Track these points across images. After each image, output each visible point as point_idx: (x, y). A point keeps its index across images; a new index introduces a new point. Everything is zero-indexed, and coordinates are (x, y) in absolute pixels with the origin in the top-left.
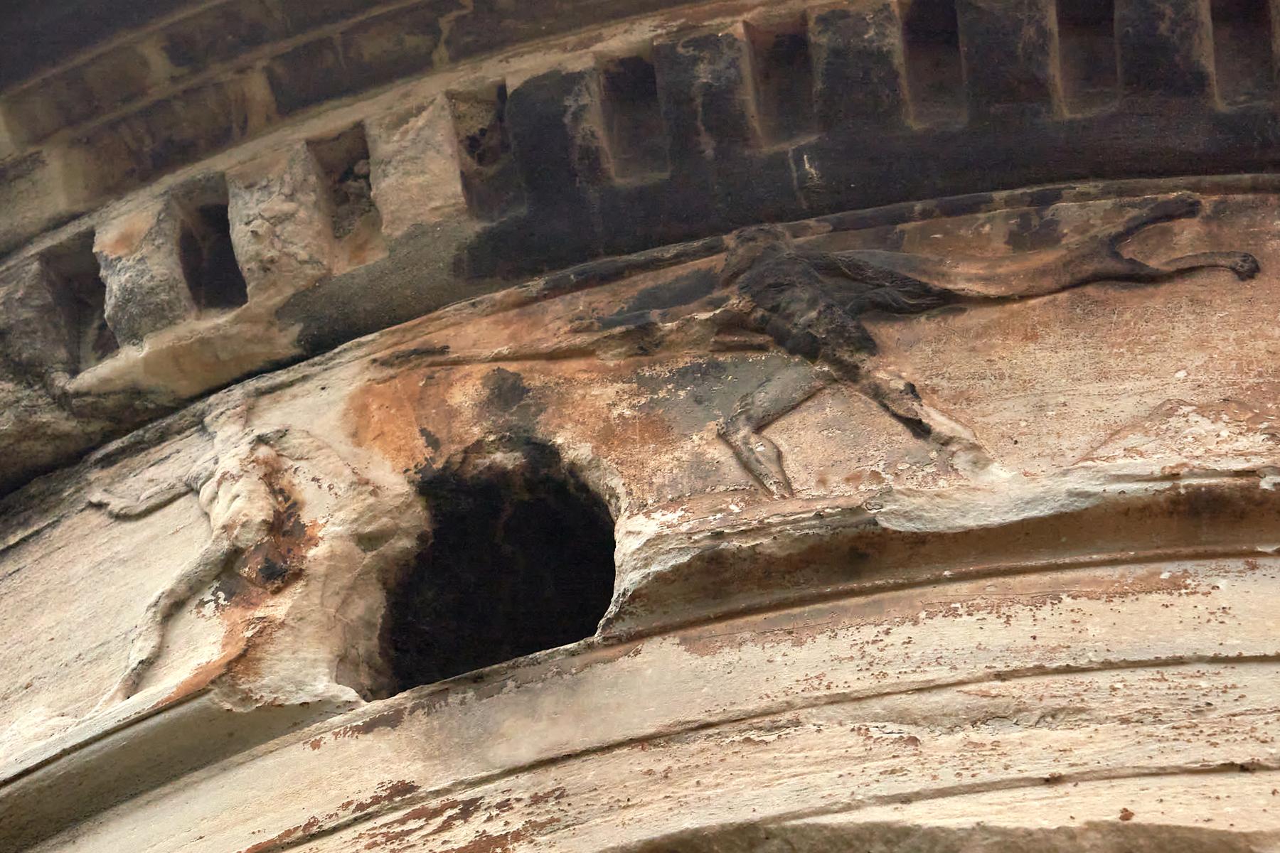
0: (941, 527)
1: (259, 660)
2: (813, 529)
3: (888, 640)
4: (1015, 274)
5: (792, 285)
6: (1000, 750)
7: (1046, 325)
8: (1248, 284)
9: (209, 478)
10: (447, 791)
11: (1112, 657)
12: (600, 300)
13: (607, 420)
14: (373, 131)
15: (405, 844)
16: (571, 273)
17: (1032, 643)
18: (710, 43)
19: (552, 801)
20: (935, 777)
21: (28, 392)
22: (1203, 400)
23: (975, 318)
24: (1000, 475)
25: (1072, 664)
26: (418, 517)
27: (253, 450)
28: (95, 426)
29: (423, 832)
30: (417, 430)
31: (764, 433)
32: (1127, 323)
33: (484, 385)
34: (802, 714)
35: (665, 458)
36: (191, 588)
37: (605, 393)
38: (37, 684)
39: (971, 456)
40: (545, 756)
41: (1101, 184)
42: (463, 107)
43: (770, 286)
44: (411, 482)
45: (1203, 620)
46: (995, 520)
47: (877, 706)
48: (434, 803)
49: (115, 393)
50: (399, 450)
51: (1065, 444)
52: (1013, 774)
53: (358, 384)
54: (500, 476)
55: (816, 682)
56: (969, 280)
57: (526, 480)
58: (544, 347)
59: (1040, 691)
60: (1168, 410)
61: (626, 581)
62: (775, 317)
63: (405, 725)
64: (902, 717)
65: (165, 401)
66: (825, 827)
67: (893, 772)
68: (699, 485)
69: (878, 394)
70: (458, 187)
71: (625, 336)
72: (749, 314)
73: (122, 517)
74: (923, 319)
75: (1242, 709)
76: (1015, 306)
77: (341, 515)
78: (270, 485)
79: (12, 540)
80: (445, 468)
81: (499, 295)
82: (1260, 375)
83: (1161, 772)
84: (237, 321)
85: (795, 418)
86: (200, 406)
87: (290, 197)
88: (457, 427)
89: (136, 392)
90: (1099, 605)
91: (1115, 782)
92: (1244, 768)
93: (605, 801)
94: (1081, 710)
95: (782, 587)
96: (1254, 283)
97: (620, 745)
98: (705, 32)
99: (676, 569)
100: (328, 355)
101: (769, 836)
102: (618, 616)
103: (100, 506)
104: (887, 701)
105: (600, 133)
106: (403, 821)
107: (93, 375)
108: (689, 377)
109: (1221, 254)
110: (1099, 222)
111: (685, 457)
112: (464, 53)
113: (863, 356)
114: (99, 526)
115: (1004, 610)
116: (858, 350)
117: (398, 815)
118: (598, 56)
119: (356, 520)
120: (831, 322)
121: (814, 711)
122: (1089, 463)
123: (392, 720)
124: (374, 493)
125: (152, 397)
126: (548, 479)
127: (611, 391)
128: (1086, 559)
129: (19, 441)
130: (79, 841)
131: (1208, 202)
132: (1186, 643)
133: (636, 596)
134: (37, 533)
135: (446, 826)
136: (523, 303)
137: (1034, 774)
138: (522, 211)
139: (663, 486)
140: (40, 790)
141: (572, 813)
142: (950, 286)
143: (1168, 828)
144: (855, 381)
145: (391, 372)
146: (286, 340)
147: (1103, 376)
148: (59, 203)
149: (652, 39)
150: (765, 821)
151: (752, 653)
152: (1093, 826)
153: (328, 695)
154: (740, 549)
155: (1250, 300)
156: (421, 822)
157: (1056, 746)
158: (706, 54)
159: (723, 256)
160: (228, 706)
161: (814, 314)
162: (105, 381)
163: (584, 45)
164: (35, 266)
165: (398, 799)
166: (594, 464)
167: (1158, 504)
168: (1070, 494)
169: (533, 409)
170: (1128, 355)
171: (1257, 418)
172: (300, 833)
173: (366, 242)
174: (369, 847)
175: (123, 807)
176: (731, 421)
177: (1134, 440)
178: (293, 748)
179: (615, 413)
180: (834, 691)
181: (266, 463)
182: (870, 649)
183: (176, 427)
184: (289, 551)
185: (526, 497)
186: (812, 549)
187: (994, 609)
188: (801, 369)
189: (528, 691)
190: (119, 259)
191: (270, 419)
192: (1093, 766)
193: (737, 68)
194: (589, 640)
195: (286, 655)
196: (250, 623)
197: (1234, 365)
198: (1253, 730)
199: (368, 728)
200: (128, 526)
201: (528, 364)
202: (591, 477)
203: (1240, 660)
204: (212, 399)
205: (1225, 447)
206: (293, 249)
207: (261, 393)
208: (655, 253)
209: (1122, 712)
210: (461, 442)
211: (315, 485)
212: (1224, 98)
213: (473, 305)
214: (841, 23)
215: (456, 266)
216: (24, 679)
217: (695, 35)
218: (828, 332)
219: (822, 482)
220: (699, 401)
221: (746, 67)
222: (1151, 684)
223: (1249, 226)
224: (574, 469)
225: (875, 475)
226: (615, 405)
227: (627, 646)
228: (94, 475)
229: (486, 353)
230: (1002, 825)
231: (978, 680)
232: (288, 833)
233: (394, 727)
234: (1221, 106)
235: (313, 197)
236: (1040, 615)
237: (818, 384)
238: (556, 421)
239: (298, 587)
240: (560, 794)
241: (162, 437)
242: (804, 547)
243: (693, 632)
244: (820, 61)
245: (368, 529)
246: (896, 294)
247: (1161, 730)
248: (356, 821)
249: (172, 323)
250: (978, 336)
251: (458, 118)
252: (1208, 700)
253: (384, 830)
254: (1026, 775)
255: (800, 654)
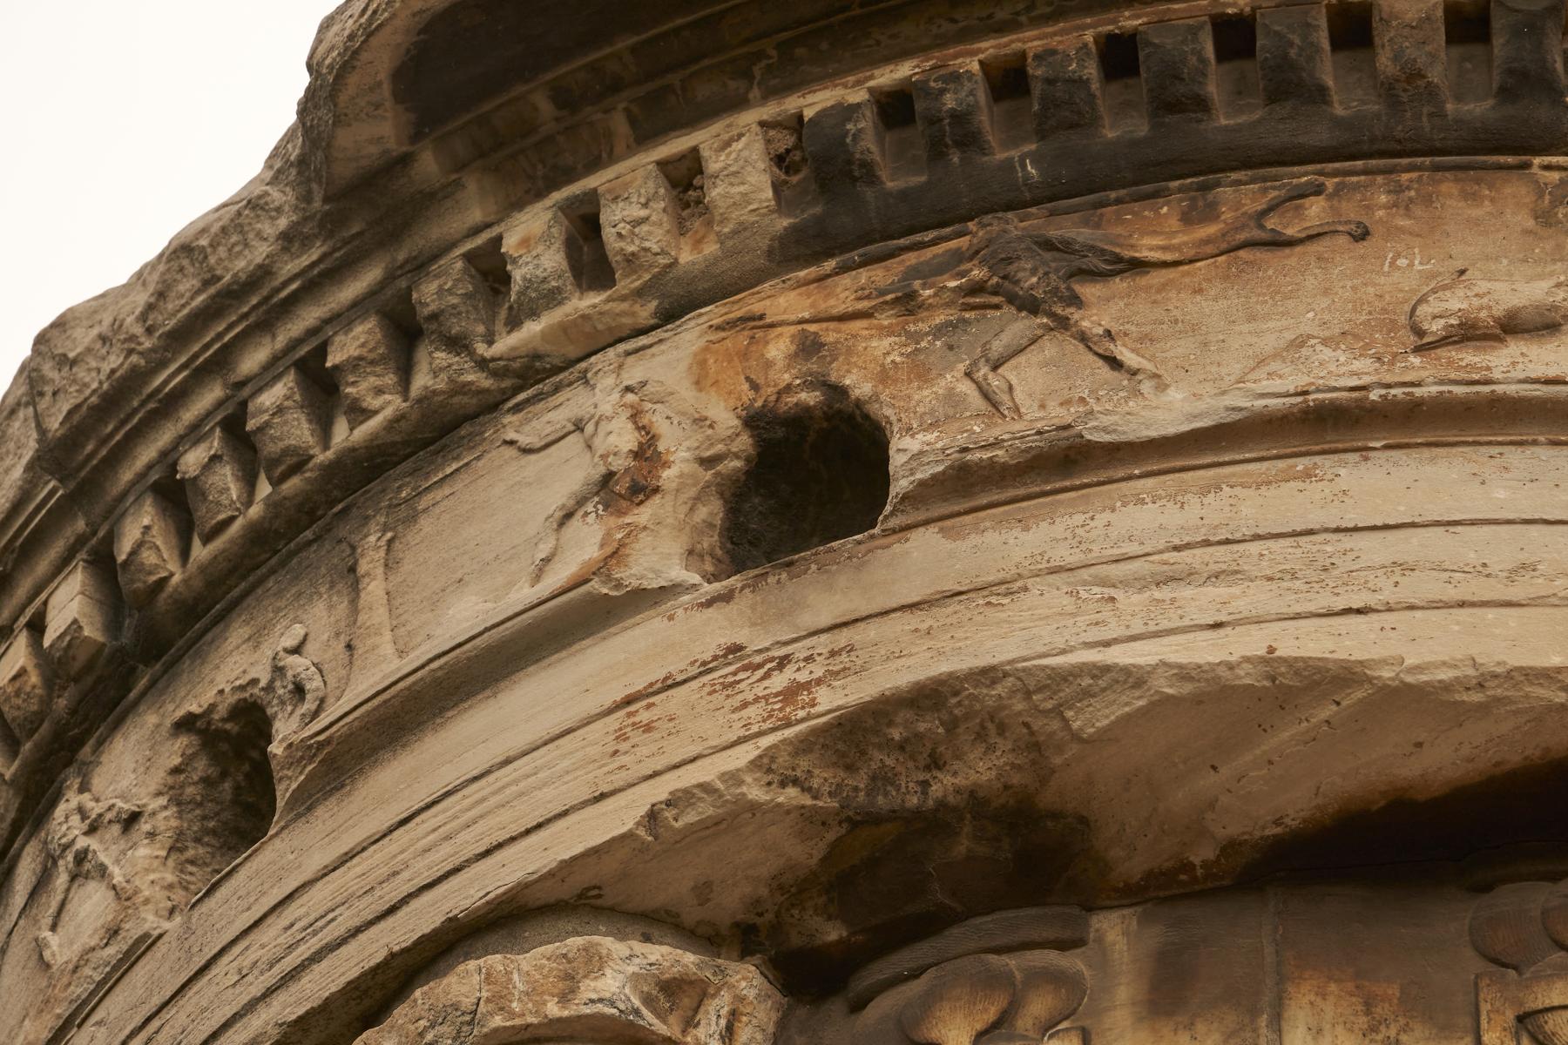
0: (1131, 437)
1: (628, 555)
2: (1035, 442)
3: (1092, 524)
4: (1185, 244)
5: (1019, 258)
6: (1177, 604)
7: (1209, 280)
8: (1360, 245)
9: (590, 420)
10: (767, 649)
11: (1260, 531)
12: (878, 275)
13: (883, 365)
14: (705, 153)
15: (736, 690)
16: (855, 256)
17: (1200, 523)
18: (955, 78)
19: (844, 655)
20: (1128, 627)
21: (457, 359)
22: (1327, 334)
23: (1157, 277)
24: (1175, 395)
25: (1230, 537)
26: (744, 442)
27: (622, 396)
28: (507, 383)
29: (750, 681)
30: (743, 377)
31: (1000, 371)
32: (1270, 278)
33: (792, 342)
34: (1030, 582)
35: (926, 393)
36: (578, 502)
37: (881, 345)
38: (466, 578)
39: (1153, 383)
40: (839, 621)
41: (1249, 173)
42: (772, 133)
43: (1002, 259)
44: (739, 417)
45: (1329, 500)
46: (1171, 430)
47: (1085, 574)
48: (758, 659)
49: (521, 357)
50: (730, 393)
51: (1224, 371)
52: (1186, 622)
53: (702, 343)
54: (804, 412)
55: (1039, 558)
56: (1151, 249)
57: (824, 413)
58: (835, 312)
59: (1207, 559)
60: (1300, 343)
61: (900, 485)
62: (1006, 283)
63: (736, 600)
64: (1104, 582)
65: (557, 362)
66: (1047, 667)
67: (1097, 624)
68: (951, 412)
69: (1083, 338)
70: (770, 194)
71: (896, 300)
72: (986, 282)
73: (527, 451)
74: (1117, 280)
75: (1358, 567)
76: (1186, 268)
77: (687, 444)
78: (635, 423)
79: (448, 471)
80: (763, 406)
81: (802, 274)
82: (1370, 313)
83: (1297, 617)
84: (608, 300)
85: (1021, 359)
86: (583, 365)
87: (645, 205)
88: (772, 374)
89: (536, 356)
90: (1251, 492)
91: (1262, 625)
92: (1359, 611)
93: (883, 652)
94: (1237, 572)
95: (1015, 487)
96: (1365, 243)
97: (894, 610)
98: (951, 69)
99: (934, 477)
100: (678, 323)
101: (1006, 675)
102: (892, 513)
103: (512, 443)
104: (1092, 570)
105: (873, 148)
106: (735, 674)
107: (506, 343)
108: (944, 331)
109: (1340, 222)
110: (1248, 202)
111: (941, 392)
112: (771, 93)
113: (1072, 310)
114: (512, 458)
115: (1179, 498)
116: (1069, 305)
117: (732, 668)
118: (870, 90)
119: (698, 447)
120: (1048, 285)
121: (1038, 579)
122: (1241, 385)
123: (726, 597)
124: (711, 426)
125: (548, 359)
126: (840, 411)
127: (886, 342)
128: (1241, 457)
129: (452, 396)
130: (499, 696)
131: (1330, 183)
132: (1315, 519)
133: (905, 498)
134: (467, 464)
135: (767, 676)
136: (821, 279)
137: (1202, 622)
138: (818, 210)
139: (925, 413)
140: (468, 659)
141: (859, 662)
142: (1137, 255)
143: (1303, 659)
144: (1067, 329)
145: (723, 334)
146: (645, 312)
147: (1252, 318)
148: (476, 215)
149: (911, 76)
150: (1002, 664)
151: (992, 538)
152: (1247, 659)
153: (679, 580)
154: (981, 460)
155: (1362, 257)
156: (748, 674)
157: (1218, 600)
158: (952, 86)
159: (968, 237)
160: (605, 591)
161: (1034, 280)
162: (513, 349)
163: (859, 83)
164: (459, 265)
165: (731, 657)
166: (875, 397)
167: (1293, 414)
168: (1227, 409)
169: (828, 359)
170: (1270, 301)
171: (1367, 346)
172: (659, 685)
173: (703, 237)
174: (710, 694)
175: (531, 669)
176: (975, 363)
177: (1274, 366)
178: (656, 620)
179: (889, 360)
180: (1052, 564)
181: (632, 407)
182: (1080, 531)
183: (566, 382)
184: (650, 472)
185: (825, 425)
186: (1035, 458)
187: (1171, 497)
188: (1026, 322)
189: (826, 572)
190: (521, 256)
191: (635, 372)
192: (1245, 614)
193: (974, 95)
194: (872, 532)
195: (647, 551)
196: (620, 527)
197: (1350, 306)
198: (1366, 582)
199: (709, 603)
200: (533, 457)
201: (824, 325)
202: (873, 409)
203: (1356, 529)
204: (593, 359)
205: (1343, 369)
206: (647, 244)
207: (628, 354)
208: (917, 238)
209: (1268, 572)
210: (775, 386)
211: (668, 421)
212: (1341, 103)
213: (784, 282)
214: (1051, 59)
215: (770, 252)
216: (459, 575)
217: (943, 72)
218: (1045, 292)
219: (1042, 406)
220: (951, 348)
221: (982, 96)
222: (1290, 550)
223: (1361, 201)
224: (858, 403)
225: (1082, 400)
226: (888, 353)
227: (900, 535)
228: (508, 419)
229: (793, 318)
230: (1179, 661)
231: (1161, 552)
232: (651, 685)
233: (728, 602)
234: (1339, 110)
235: (662, 205)
236: (1206, 501)
237: (1039, 332)
238: (846, 367)
239: (657, 499)
240: (850, 649)
241: (557, 389)
242: (1029, 456)
243: (948, 523)
244: (1037, 89)
245: (708, 454)
246: (1095, 261)
247: (1298, 584)
248: (701, 674)
249: (560, 303)
250: (1159, 291)
251: (768, 142)
252: (1333, 560)
253: (721, 680)
254: (1196, 622)
255: (1024, 536)
